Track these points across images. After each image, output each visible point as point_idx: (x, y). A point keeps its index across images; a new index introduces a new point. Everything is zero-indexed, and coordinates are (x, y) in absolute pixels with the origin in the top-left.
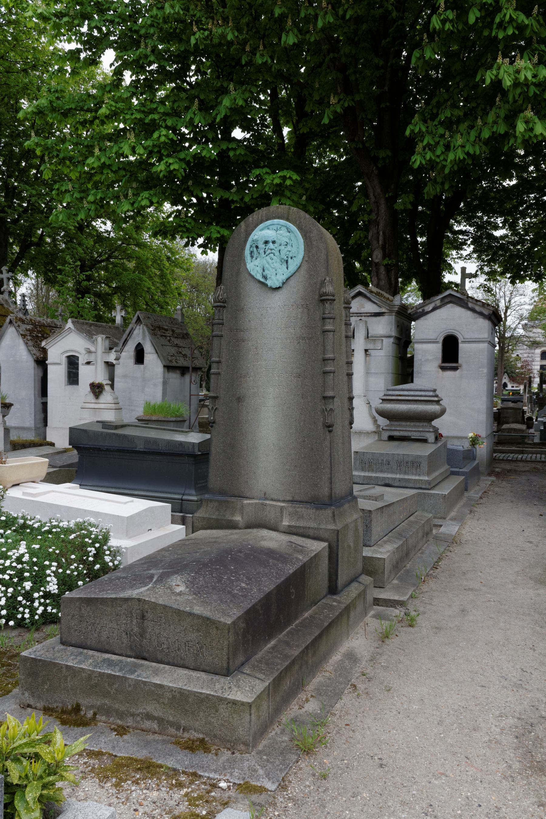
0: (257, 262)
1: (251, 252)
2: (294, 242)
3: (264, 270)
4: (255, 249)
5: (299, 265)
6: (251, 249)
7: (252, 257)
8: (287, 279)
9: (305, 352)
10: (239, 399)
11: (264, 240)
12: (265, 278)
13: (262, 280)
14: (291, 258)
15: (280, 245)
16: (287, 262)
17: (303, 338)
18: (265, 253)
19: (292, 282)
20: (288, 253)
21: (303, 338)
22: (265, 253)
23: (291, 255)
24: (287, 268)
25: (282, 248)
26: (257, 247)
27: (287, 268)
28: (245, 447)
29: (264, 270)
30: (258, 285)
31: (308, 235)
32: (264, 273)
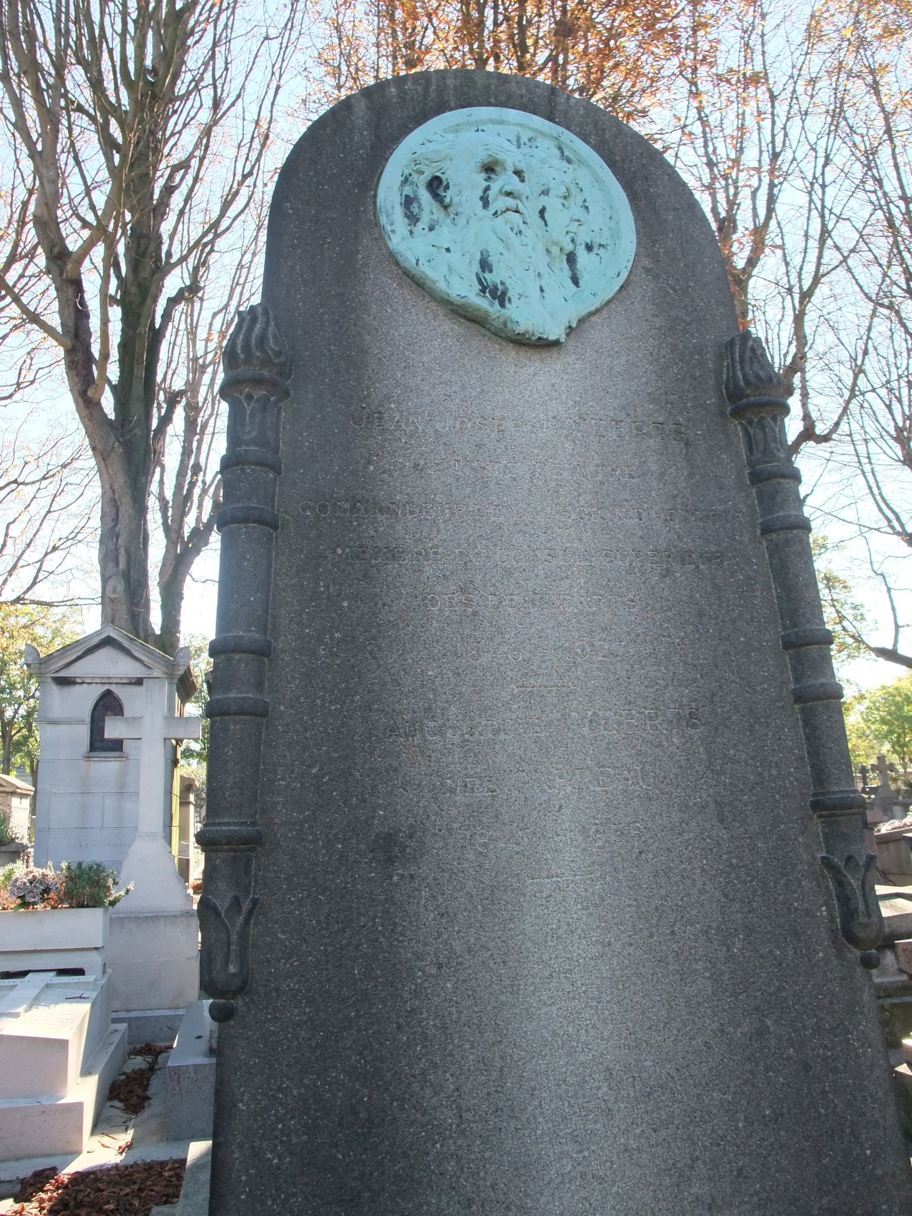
0: (445, 234)
1: (408, 202)
2: (592, 194)
3: (485, 265)
4: (425, 196)
5: (624, 275)
6: (408, 190)
7: (413, 219)
8: (581, 321)
9: (701, 614)
10: (391, 849)
11: (482, 156)
12: (500, 296)
13: (483, 303)
14: (589, 248)
15: (545, 192)
16: (571, 258)
17: (684, 557)
18: (485, 201)
19: (599, 333)
20: (574, 227)
21: (684, 557)
22: (485, 201)
23: (584, 237)
24: (575, 281)
25: (552, 203)
26: (436, 185)
27: (575, 281)
28: (450, 1117)
29: (485, 265)
30: (449, 325)
31: (638, 186)
32: (490, 278)
